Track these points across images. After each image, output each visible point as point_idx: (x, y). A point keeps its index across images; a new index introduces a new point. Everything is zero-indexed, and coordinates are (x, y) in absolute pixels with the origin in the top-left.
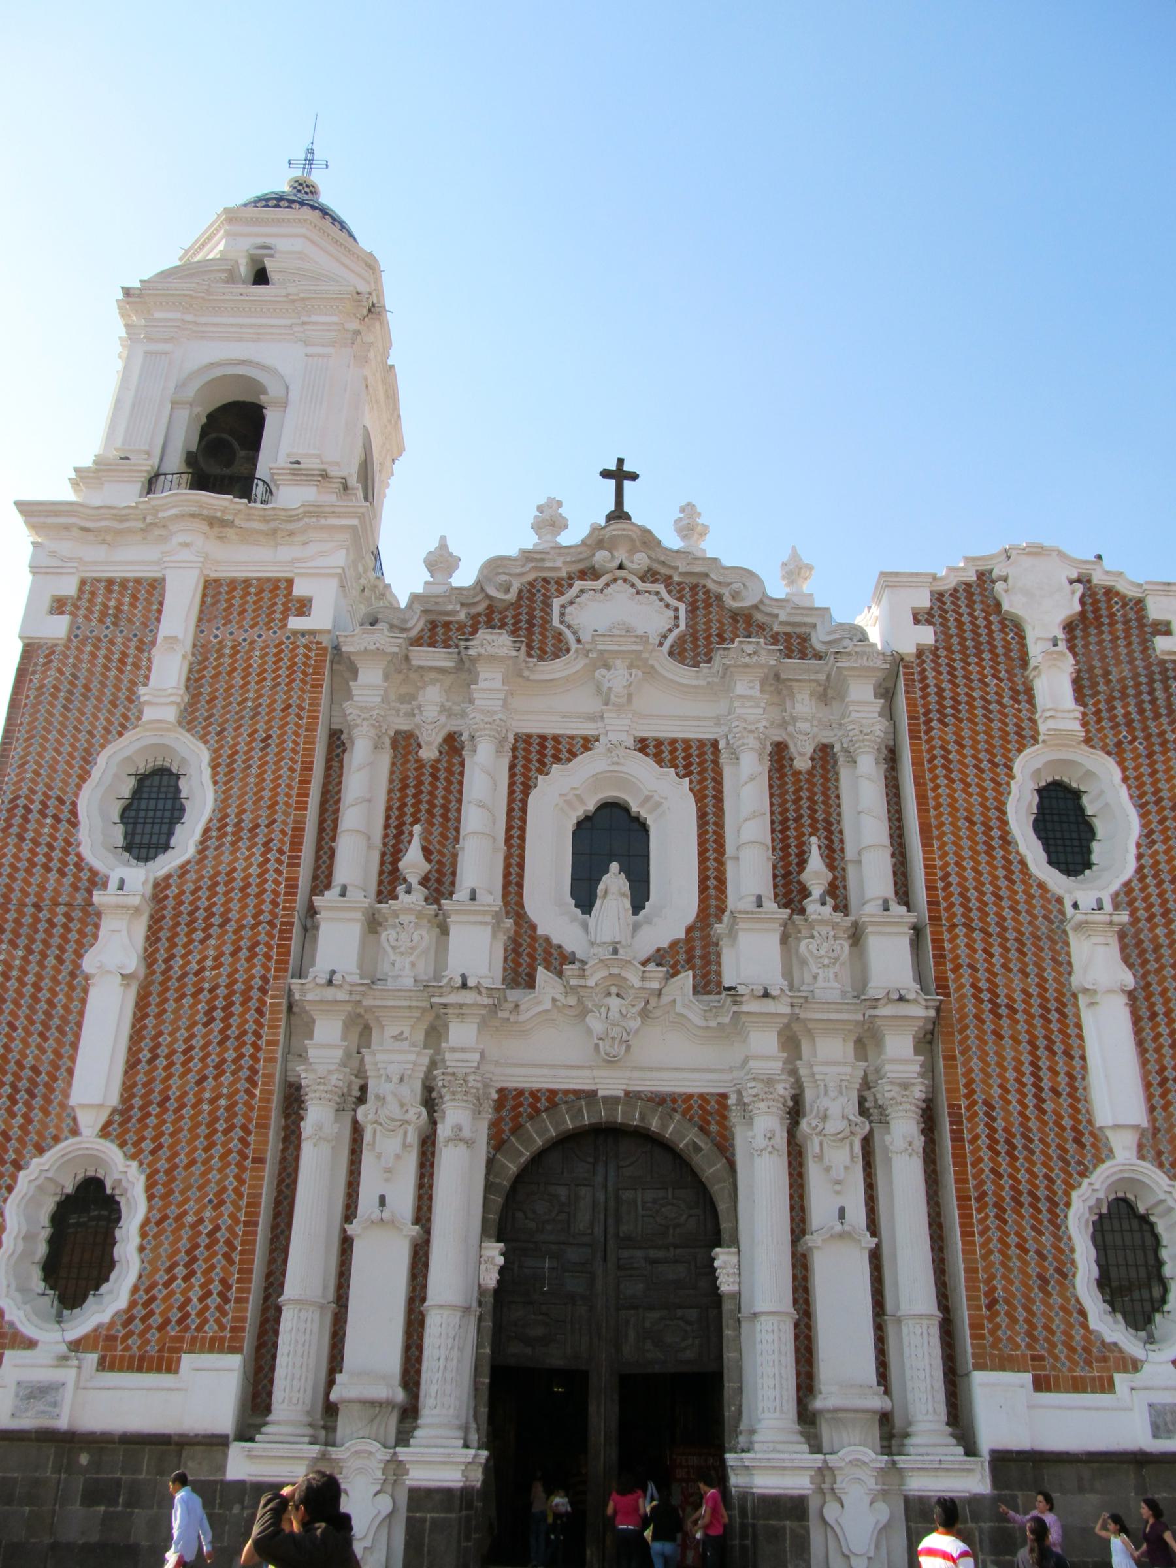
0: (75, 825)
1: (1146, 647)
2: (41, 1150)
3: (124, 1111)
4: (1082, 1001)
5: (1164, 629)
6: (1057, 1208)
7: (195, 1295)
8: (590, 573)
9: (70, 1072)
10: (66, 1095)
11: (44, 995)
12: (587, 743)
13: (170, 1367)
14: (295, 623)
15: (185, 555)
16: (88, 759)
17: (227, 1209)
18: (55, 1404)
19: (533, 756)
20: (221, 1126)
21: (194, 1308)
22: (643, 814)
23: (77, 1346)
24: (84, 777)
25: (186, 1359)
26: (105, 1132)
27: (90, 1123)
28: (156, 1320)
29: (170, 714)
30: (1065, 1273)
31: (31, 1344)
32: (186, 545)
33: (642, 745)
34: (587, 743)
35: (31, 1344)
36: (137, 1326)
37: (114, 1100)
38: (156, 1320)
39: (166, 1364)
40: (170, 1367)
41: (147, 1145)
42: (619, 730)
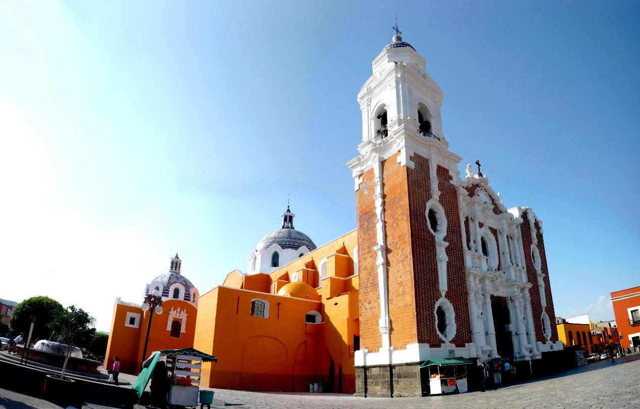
0: (426, 221)
2: (437, 300)
3: (447, 292)
9: (438, 282)
13: (464, 346)
18: (454, 354)
22: (487, 241)
23: (451, 342)
24: (425, 209)
25: (466, 344)
26: (446, 297)
27: (443, 294)
31: (444, 342)
35: (444, 342)
37: (446, 289)
40: (464, 346)
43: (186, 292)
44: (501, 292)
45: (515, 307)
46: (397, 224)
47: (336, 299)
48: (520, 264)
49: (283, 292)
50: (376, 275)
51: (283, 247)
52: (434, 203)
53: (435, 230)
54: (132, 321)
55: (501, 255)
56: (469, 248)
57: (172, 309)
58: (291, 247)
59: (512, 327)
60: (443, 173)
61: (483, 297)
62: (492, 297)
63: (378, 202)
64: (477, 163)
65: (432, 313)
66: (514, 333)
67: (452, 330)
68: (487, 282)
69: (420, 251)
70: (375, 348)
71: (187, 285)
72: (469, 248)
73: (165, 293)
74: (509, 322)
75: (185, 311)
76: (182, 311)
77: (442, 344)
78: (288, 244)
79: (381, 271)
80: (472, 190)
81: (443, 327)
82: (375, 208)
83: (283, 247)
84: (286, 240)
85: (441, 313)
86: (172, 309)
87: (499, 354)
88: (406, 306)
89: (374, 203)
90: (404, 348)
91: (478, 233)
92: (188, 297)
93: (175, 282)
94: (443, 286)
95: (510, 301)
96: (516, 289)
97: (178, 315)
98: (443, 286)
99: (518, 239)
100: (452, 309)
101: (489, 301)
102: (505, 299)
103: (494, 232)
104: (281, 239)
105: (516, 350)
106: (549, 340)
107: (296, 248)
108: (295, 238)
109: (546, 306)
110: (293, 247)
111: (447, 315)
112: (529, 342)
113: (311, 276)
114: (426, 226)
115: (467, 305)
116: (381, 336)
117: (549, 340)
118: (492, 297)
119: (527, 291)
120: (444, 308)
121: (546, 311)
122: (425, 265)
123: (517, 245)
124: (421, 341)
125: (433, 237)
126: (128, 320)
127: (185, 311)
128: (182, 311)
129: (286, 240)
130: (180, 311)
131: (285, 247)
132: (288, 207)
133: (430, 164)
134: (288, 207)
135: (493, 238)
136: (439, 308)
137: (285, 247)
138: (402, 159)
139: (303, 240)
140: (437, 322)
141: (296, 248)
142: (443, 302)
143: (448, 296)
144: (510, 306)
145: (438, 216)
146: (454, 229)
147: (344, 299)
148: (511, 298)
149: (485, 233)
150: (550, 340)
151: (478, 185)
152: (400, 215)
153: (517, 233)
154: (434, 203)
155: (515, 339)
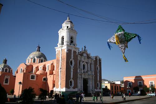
5: (101, 61)
12: (84, 62)
19: (83, 62)
27: (72, 78)
34: (84, 62)
44: (86, 77)
48: (93, 70)
49: (38, 73)
50: (59, 74)
52: (72, 59)
53: (71, 65)
56: (79, 68)
62: (83, 78)
63: (60, 58)
64: (85, 47)
70: (58, 87)
71: (9, 68)
72: (79, 68)
79: (60, 73)
80: (81, 54)
81: (71, 85)
85: (71, 82)
87: (83, 91)
90: (63, 88)
91: (82, 64)
94: (72, 77)
98: (72, 77)
99: (93, 64)
101: (82, 79)
102: (88, 78)
103: (87, 63)
112: (92, 89)
113: (44, 68)
118: (83, 78)
120: (72, 81)
124: (66, 87)
135: (86, 64)
136: (71, 81)
138: (66, 50)
142: (72, 80)
144: (89, 80)
146: (76, 65)
147: (52, 76)
151: (84, 53)
153: (93, 62)
154: (72, 59)
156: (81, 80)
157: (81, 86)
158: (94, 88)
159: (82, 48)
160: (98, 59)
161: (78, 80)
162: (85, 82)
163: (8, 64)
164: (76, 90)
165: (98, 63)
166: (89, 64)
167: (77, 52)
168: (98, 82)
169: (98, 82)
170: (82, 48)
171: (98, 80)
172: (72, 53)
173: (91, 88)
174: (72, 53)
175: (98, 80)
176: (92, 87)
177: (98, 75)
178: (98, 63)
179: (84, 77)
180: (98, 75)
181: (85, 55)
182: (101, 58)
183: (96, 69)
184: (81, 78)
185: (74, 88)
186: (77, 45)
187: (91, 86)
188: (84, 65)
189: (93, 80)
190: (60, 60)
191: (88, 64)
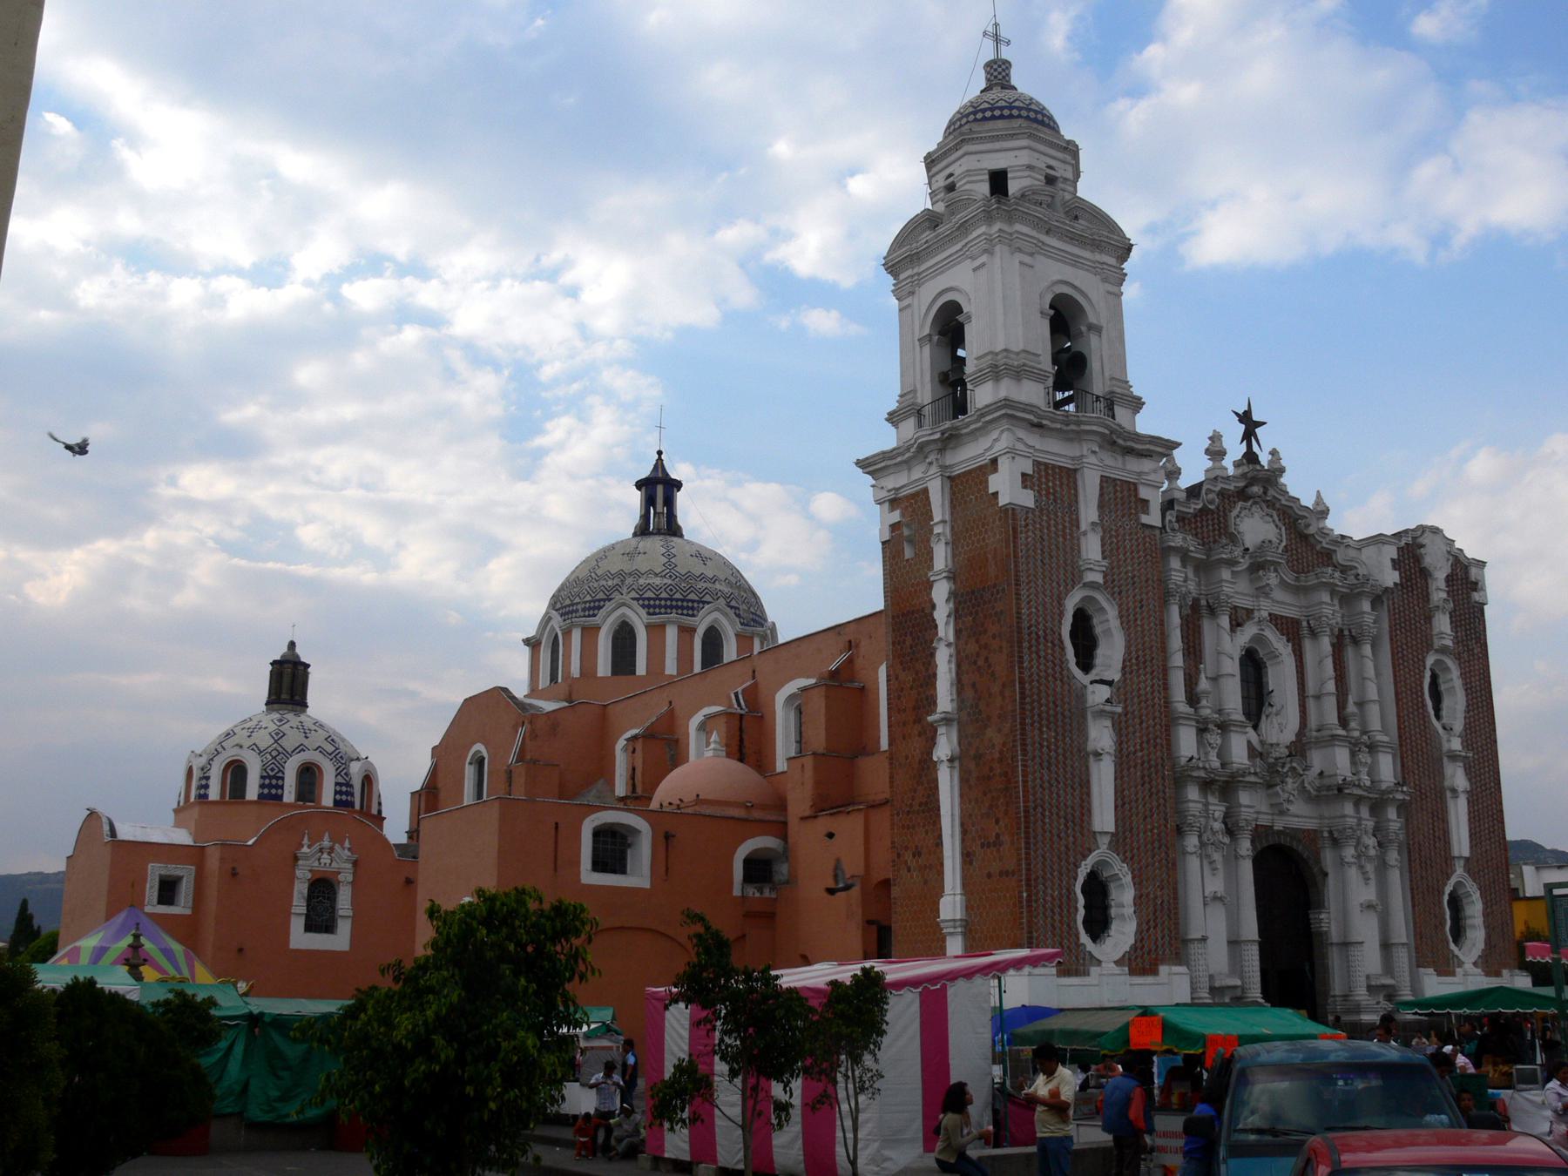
0: (1063, 649)
1: (1469, 597)
2: (1085, 857)
4: (1449, 794)
6: (1441, 893)
7: (1159, 935)
8: (1242, 494)
9: (1089, 811)
10: (1090, 823)
11: (1069, 762)
14: (1145, 519)
15: (1093, 459)
16: (1060, 604)
17: (1166, 891)
20: (1156, 844)
21: (1160, 942)
23: (1117, 963)
24: (1061, 615)
27: (1104, 842)
28: (1146, 949)
29: (1099, 578)
30: (1443, 924)
31: (1099, 963)
32: (1094, 452)
33: (1275, 619)
36: (1139, 952)
37: (1112, 829)
38: (1146, 949)
39: (1152, 970)
41: (1128, 854)
42: (1265, 608)
43: (340, 780)
44: (1300, 816)
45: (1342, 863)
46: (987, 659)
47: (824, 824)
51: (649, 606)
54: (168, 891)
55: (1311, 704)
57: (306, 841)
58: (677, 607)
59: (1328, 921)
60: (1121, 498)
61: (1227, 840)
62: (1259, 833)
63: (941, 592)
65: (1070, 891)
66: (1335, 937)
67: (1123, 934)
68: (1244, 798)
69: (1042, 732)
72: (1193, 699)
73: (270, 786)
74: (1321, 905)
75: (347, 844)
76: (337, 846)
77: (1094, 970)
78: (664, 595)
82: (933, 607)
83: (649, 606)
84: (658, 581)
85: (1097, 889)
86: (306, 841)
88: (1004, 873)
89: (931, 587)
92: (347, 793)
93: (301, 749)
94: (1104, 817)
95: (1327, 843)
96: (1349, 809)
97: (325, 858)
98: (1104, 817)
100: (1128, 879)
101: (1245, 847)
102: (1312, 836)
103: (1291, 629)
104: (641, 581)
105: (1337, 988)
106: (1469, 966)
107: (692, 608)
108: (689, 575)
109: (1466, 853)
110: (682, 608)
111: (1114, 894)
112: (1388, 967)
114: (1063, 662)
115: (1174, 864)
116: (944, 941)
117: (1469, 966)
119: (1392, 813)
121: (1468, 870)
122: (1053, 768)
123: (1369, 665)
125: (1081, 696)
126: (152, 891)
127: (347, 844)
128: (337, 846)
129: (658, 581)
130: (331, 850)
131: (655, 607)
132: (660, 453)
133: (1080, 483)
134: (660, 453)
136: (1093, 876)
137: (655, 607)
139: (714, 580)
140: (1081, 912)
141: (692, 608)
143: (1119, 841)
144: (1328, 857)
145: (1098, 630)
146: (1145, 659)
148: (1331, 832)
149: (1259, 638)
150: (1475, 964)
151: (1242, 494)
152: (994, 637)
155: (1335, 959)
156: (1233, 858)
157: (1234, 943)
158: (1402, 958)
159: (1215, 438)
160: (1440, 574)
161: (1193, 864)
162: (1288, 882)
163: (323, 701)
164: (1168, 989)
165: (1443, 624)
166: (1326, 643)
167: (1144, 493)
168: (1459, 872)
169: (1459, 872)
170: (1215, 438)
171: (1461, 842)
172: (1089, 512)
173: (1369, 961)
174: (1089, 512)
175: (1461, 842)
176: (1386, 946)
177: (1457, 777)
178: (1443, 624)
179: (1264, 820)
180: (1457, 777)
181: (1255, 528)
182: (1471, 553)
183: (1416, 701)
184: (1231, 831)
185: (1141, 962)
186: (1137, 404)
187: (1366, 930)
188: (1253, 665)
189: (1393, 856)
190: (942, 613)
191: (1307, 644)
